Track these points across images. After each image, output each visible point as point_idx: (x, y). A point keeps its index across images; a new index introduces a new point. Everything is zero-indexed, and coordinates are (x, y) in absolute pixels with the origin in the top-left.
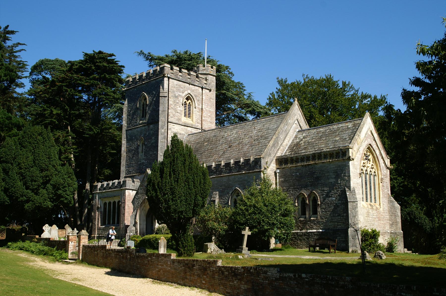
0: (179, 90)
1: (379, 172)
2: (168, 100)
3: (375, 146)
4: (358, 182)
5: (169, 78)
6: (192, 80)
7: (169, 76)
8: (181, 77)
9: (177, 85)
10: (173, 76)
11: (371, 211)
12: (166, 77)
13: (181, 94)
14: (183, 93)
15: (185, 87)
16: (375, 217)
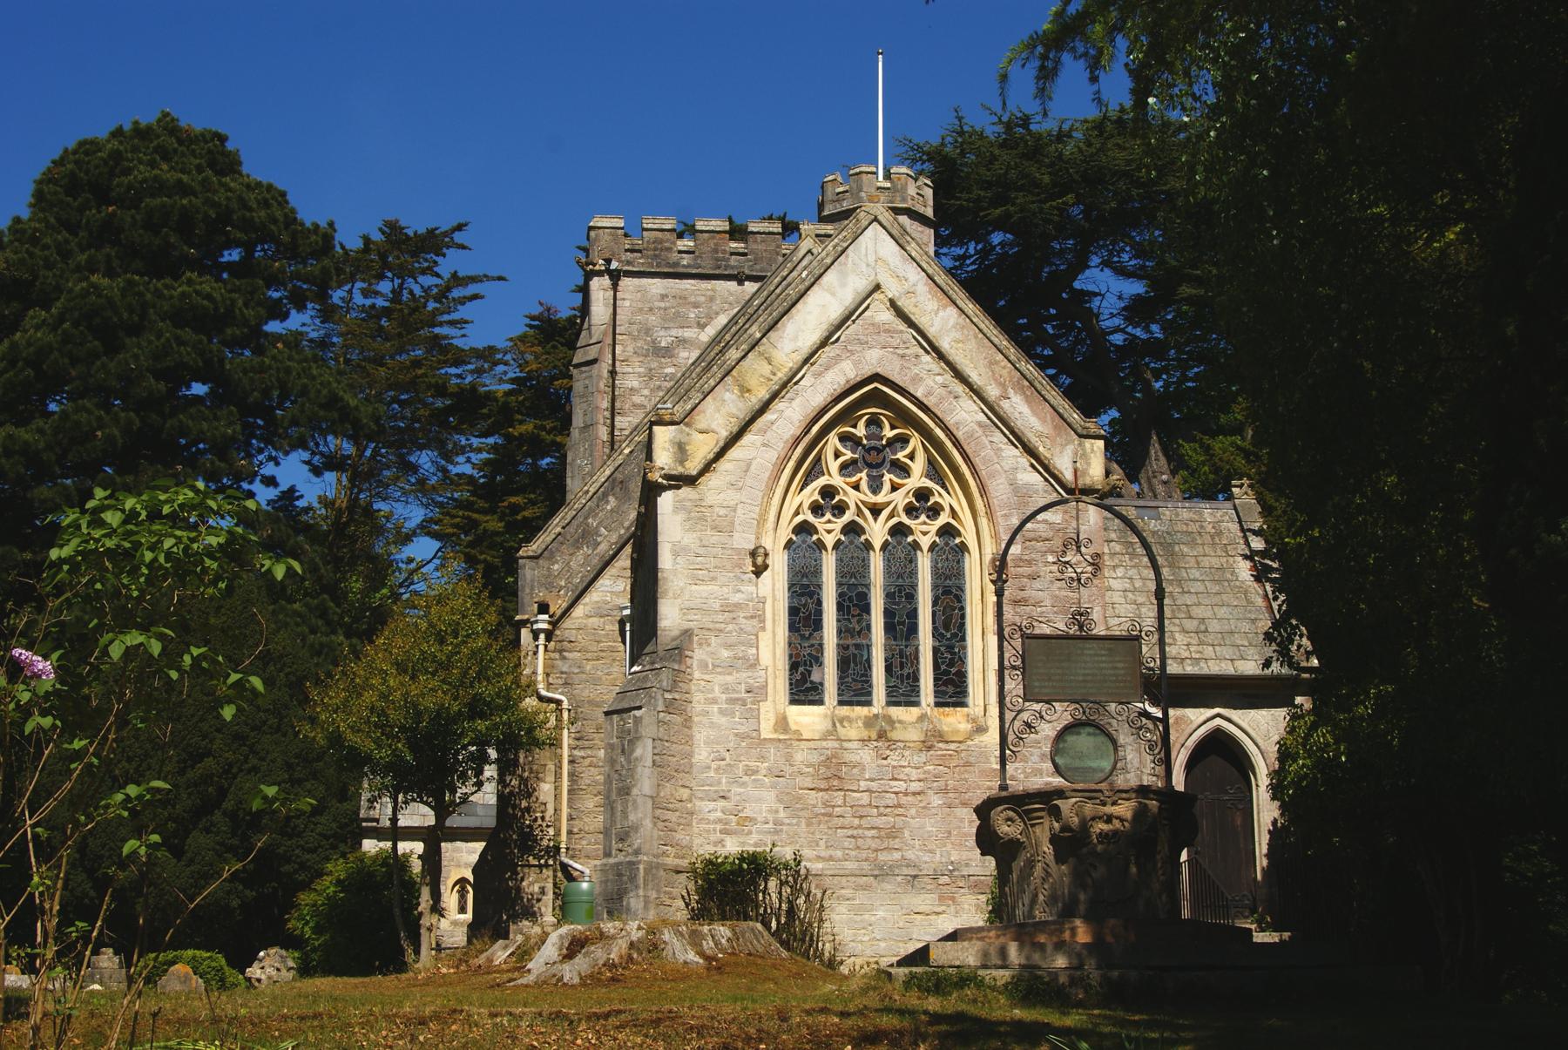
0: (677, 314)
1: (983, 522)
2: (613, 373)
3: (927, 381)
4: (737, 598)
5: (615, 276)
6: (756, 261)
7: (614, 265)
8: (686, 260)
9: (663, 297)
10: (640, 263)
11: (866, 756)
12: (600, 274)
13: (689, 333)
14: (702, 326)
15: (712, 299)
16: (915, 786)
